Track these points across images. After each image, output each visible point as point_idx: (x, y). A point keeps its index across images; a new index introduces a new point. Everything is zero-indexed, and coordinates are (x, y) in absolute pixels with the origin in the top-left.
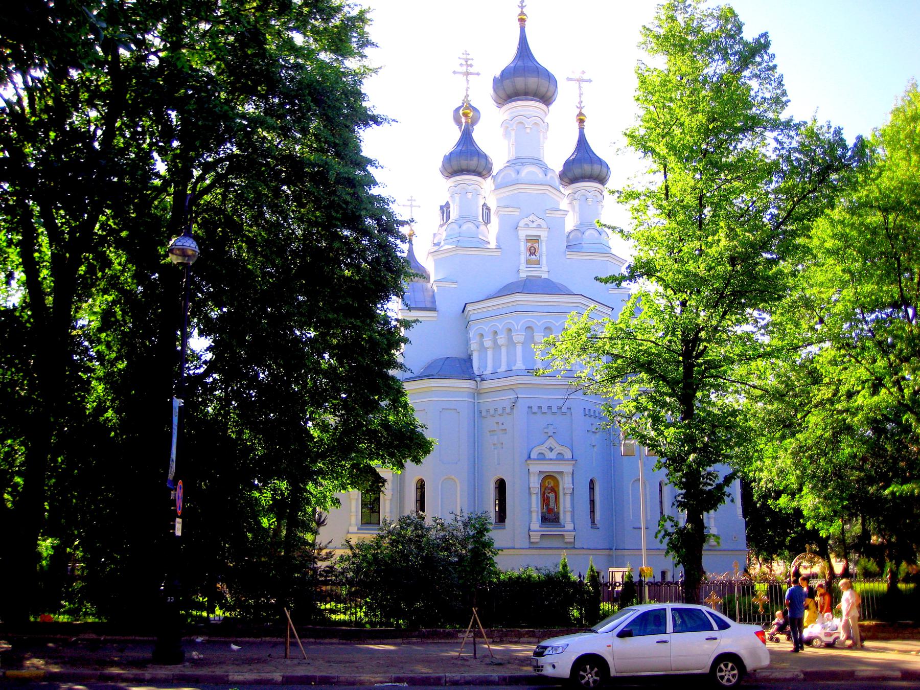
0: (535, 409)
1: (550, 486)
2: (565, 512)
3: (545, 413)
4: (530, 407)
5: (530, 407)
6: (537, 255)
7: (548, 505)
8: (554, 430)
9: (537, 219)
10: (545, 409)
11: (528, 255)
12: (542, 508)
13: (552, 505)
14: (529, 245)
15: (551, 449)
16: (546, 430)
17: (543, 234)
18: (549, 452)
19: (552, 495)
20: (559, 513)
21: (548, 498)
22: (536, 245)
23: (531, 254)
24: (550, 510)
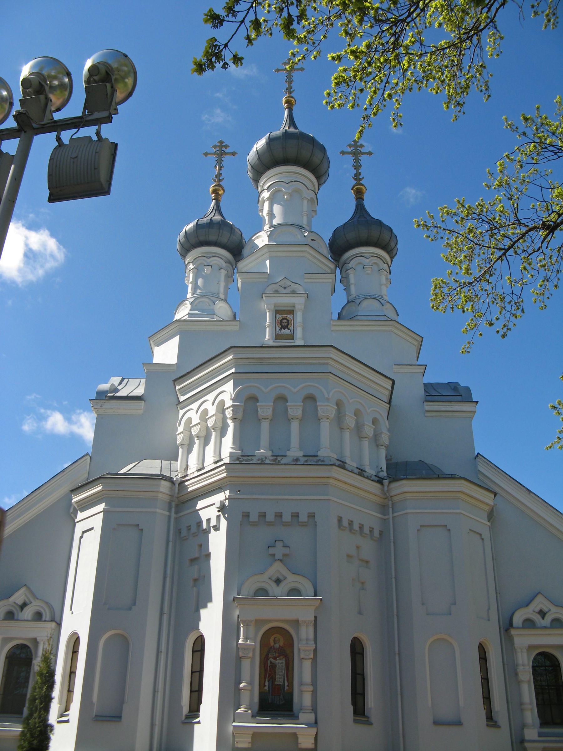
0: (254, 517)
1: (277, 646)
2: (301, 692)
3: (270, 524)
4: (246, 515)
5: (246, 515)
6: (291, 328)
7: (272, 679)
8: (286, 551)
9: (290, 283)
10: (270, 517)
11: (278, 328)
12: (262, 685)
13: (280, 679)
14: (279, 317)
15: (278, 581)
16: (272, 551)
17: (299, 302)
18: (274, 585)
19: (280, 662)
20: (291, 694)
21: (273, 666)
22: (290, 317)
23: (283, 327)
24: (276, 689)
